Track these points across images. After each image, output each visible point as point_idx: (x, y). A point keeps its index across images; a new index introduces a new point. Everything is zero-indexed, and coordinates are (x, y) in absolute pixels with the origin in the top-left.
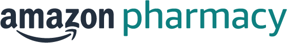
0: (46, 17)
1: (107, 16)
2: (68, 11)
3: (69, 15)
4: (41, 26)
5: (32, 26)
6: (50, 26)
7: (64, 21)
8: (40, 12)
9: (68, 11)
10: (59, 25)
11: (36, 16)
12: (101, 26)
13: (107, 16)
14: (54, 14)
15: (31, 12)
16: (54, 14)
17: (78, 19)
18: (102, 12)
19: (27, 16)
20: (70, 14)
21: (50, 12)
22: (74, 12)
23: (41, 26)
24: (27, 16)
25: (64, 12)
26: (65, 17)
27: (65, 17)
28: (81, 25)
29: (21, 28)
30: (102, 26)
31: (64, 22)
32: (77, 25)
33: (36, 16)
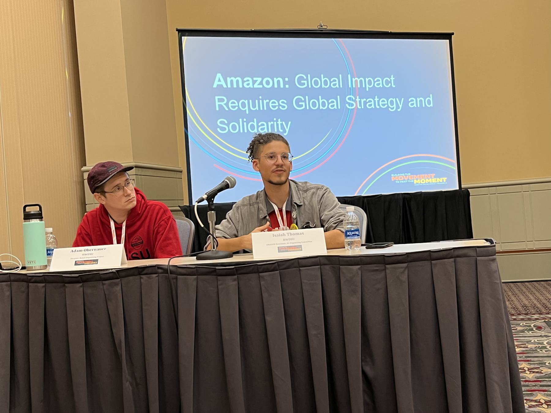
0: (243, 82)
1: (279, 82)
2: (255, 79)
3: (257, 81)
4: (241, 86)
5: (235, 86)
6: (246, 86)
7: (253, 84)
8: (240, 79)
9: (255, 79)
10: (251, 86)
11: (237, 81)
12: (276, 86)
13: (279, 82)
14: (248, 80)
15: (235, 80)
16: (248, 80)
17: (261, 83)
18: (276, 80)
19: (232, 81)
20: (257, 81)
21: (245, 79)
22: (259, 79)
23: (241, 86)
24: (232, 81)
25: (253, 79)
26: (254, 82)
27: (254, 82)
28: (263, 86)
29: (228, 87)
30: (276, 86)
31: (253, 84)
32: (261, 86)
33: (237, 81)
